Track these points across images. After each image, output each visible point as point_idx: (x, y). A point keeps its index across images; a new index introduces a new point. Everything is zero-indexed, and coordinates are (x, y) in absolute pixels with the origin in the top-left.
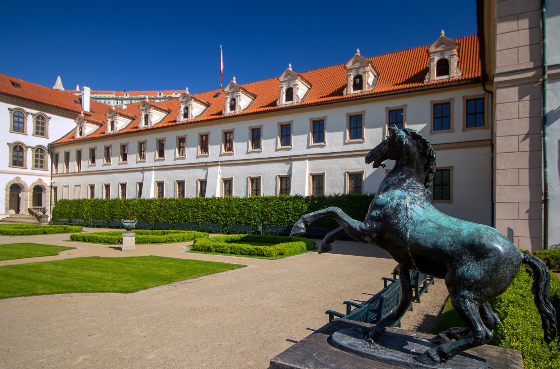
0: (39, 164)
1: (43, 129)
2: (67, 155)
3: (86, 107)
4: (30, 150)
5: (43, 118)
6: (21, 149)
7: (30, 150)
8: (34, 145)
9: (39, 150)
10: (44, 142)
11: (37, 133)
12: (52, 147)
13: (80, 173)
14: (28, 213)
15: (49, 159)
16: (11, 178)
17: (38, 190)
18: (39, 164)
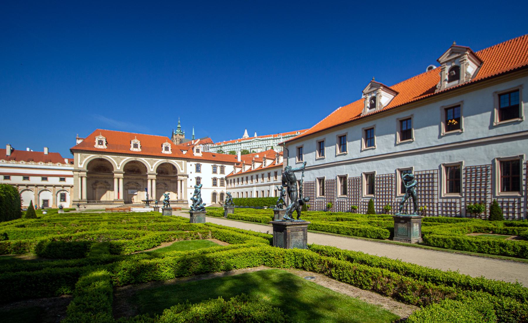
0: (222, 185)
1: (223, 171)
2: (231, 180)
3: (239, 160)
4: (219, 180)
5: (223, 167)
6: (216, 179)
7: (219, 180)
8: (220, 178)
9: (222, 179)
10: (224, 176)
11: (221, 173)
12: (226, 178)
13: (235, 188)
14: (218, 204)
15: (225, 182)
16: (212, 191)
17: (222, 195)
18: (222, 185)
